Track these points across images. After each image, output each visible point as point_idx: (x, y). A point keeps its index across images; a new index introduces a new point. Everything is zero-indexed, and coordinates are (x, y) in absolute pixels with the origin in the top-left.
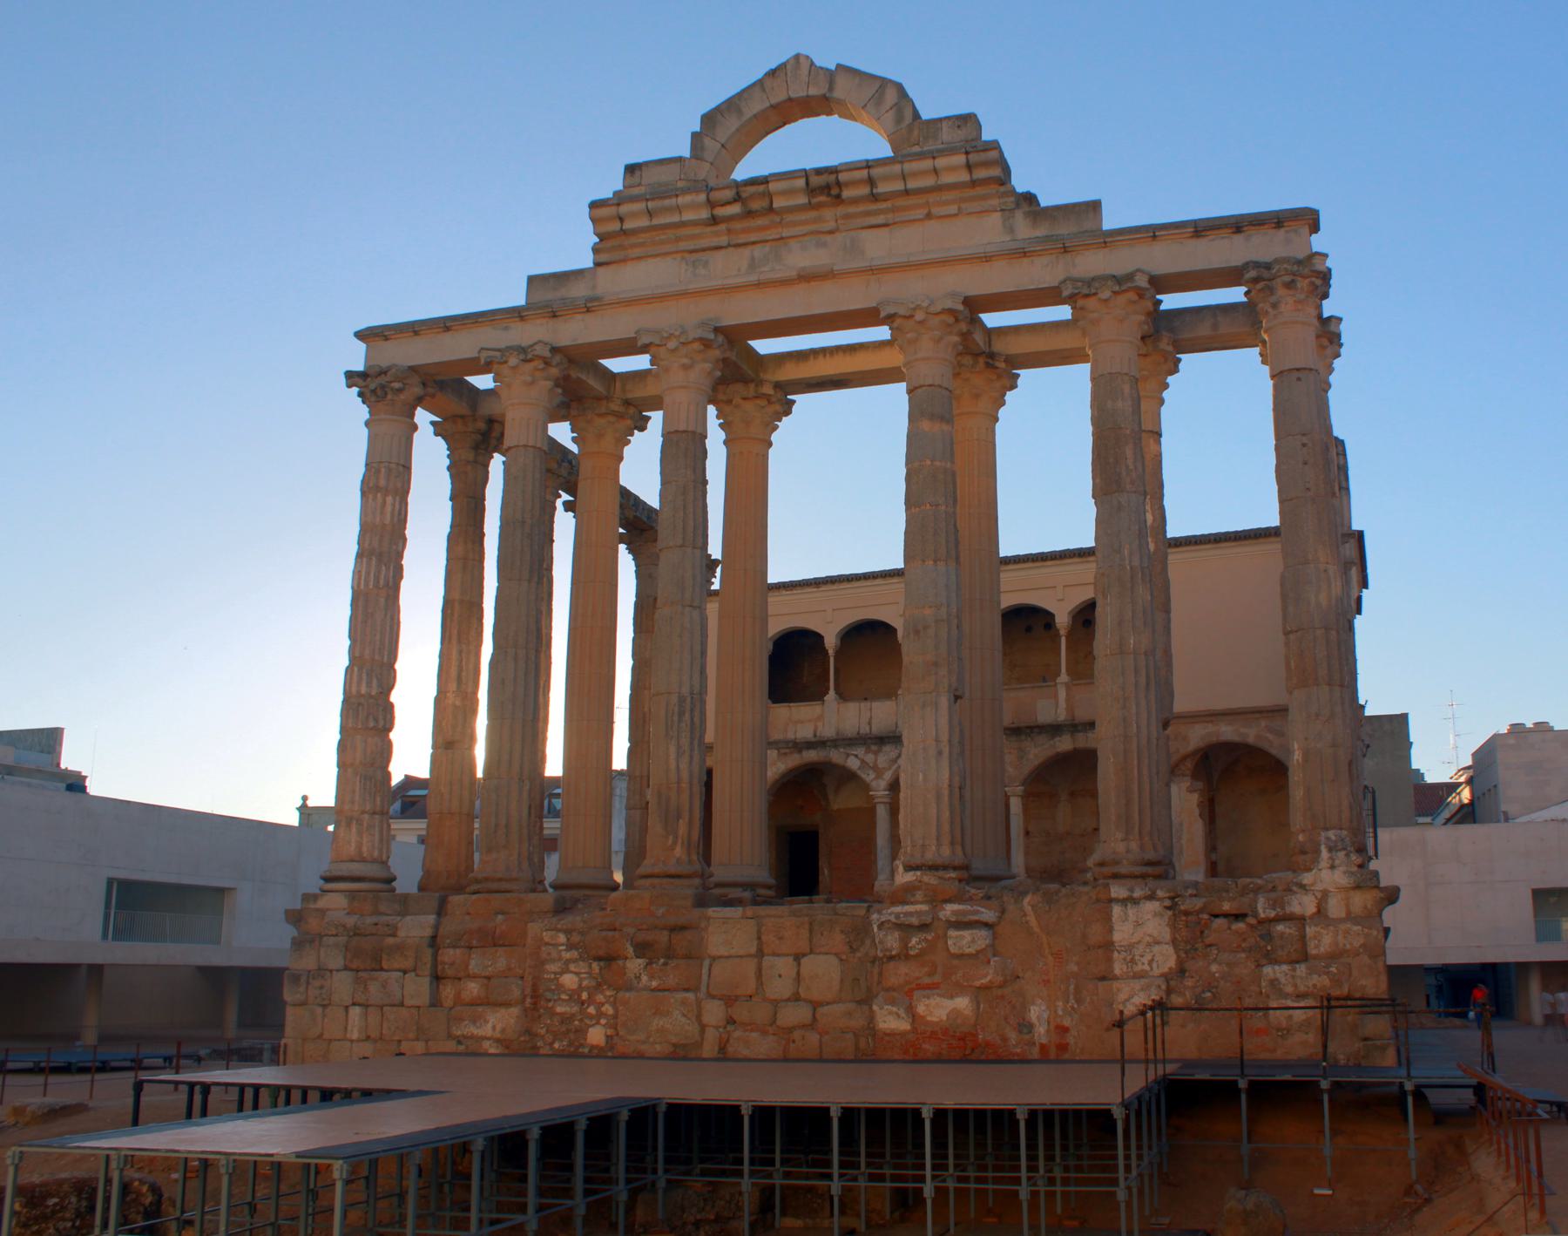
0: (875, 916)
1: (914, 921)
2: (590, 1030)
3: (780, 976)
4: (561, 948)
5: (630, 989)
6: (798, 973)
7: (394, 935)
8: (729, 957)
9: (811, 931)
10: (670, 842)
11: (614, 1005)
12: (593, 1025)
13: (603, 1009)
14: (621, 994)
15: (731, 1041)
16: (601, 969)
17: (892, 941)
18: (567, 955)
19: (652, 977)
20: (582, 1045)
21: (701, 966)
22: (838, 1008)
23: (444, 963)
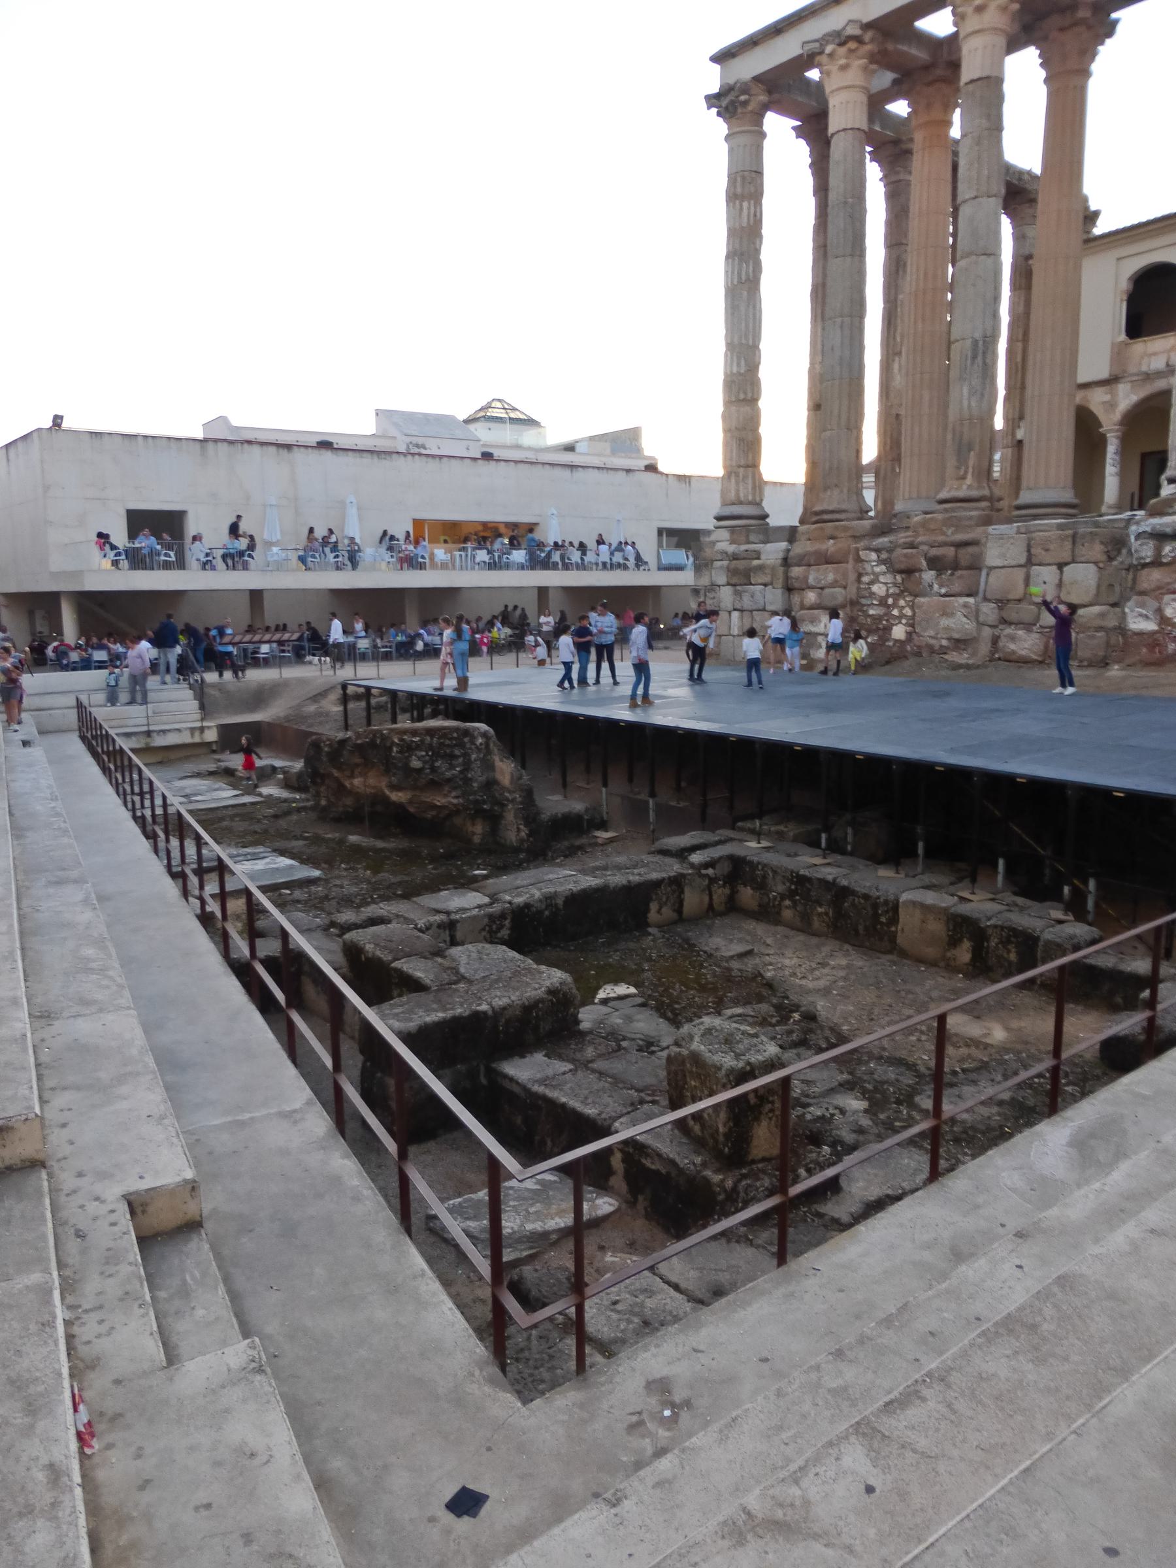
0: (1133, 528)
1: (1168, 530)
2: (895, 628)
3: (1045, 583)
5: (924, 595)
6: (1061, 580)
7: (759, 558)
8: (1004, 567)
9: (1074, 543)
10: (962, 472)
11: (912, 608)
12: (896, 625)
13: (904, 612)
15: (1002, 637)
16: (903, 579)
17: (1147, 551)
18: (877, 569)
19: (941, 586)
20: (888, 640)
21: (980, 575)
22: (1096, 609)
23: (792, 578)
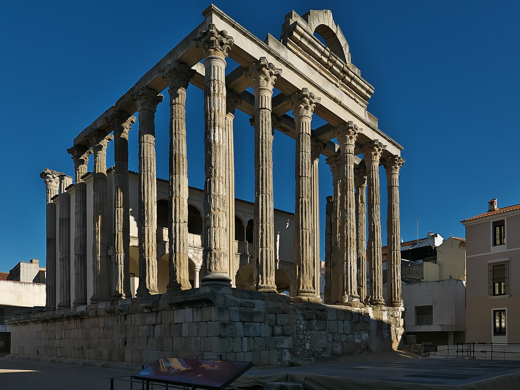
4: (300, 315)
8: (332, 320)
11: (310, 335)
14: (312, 332)
22: (350, 336)
